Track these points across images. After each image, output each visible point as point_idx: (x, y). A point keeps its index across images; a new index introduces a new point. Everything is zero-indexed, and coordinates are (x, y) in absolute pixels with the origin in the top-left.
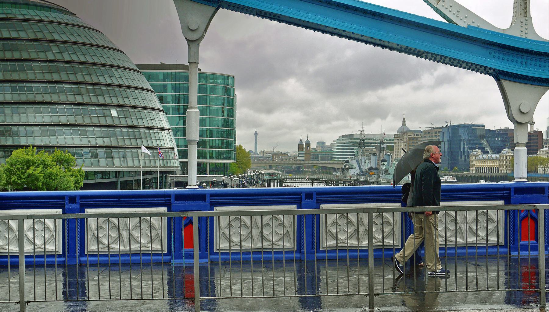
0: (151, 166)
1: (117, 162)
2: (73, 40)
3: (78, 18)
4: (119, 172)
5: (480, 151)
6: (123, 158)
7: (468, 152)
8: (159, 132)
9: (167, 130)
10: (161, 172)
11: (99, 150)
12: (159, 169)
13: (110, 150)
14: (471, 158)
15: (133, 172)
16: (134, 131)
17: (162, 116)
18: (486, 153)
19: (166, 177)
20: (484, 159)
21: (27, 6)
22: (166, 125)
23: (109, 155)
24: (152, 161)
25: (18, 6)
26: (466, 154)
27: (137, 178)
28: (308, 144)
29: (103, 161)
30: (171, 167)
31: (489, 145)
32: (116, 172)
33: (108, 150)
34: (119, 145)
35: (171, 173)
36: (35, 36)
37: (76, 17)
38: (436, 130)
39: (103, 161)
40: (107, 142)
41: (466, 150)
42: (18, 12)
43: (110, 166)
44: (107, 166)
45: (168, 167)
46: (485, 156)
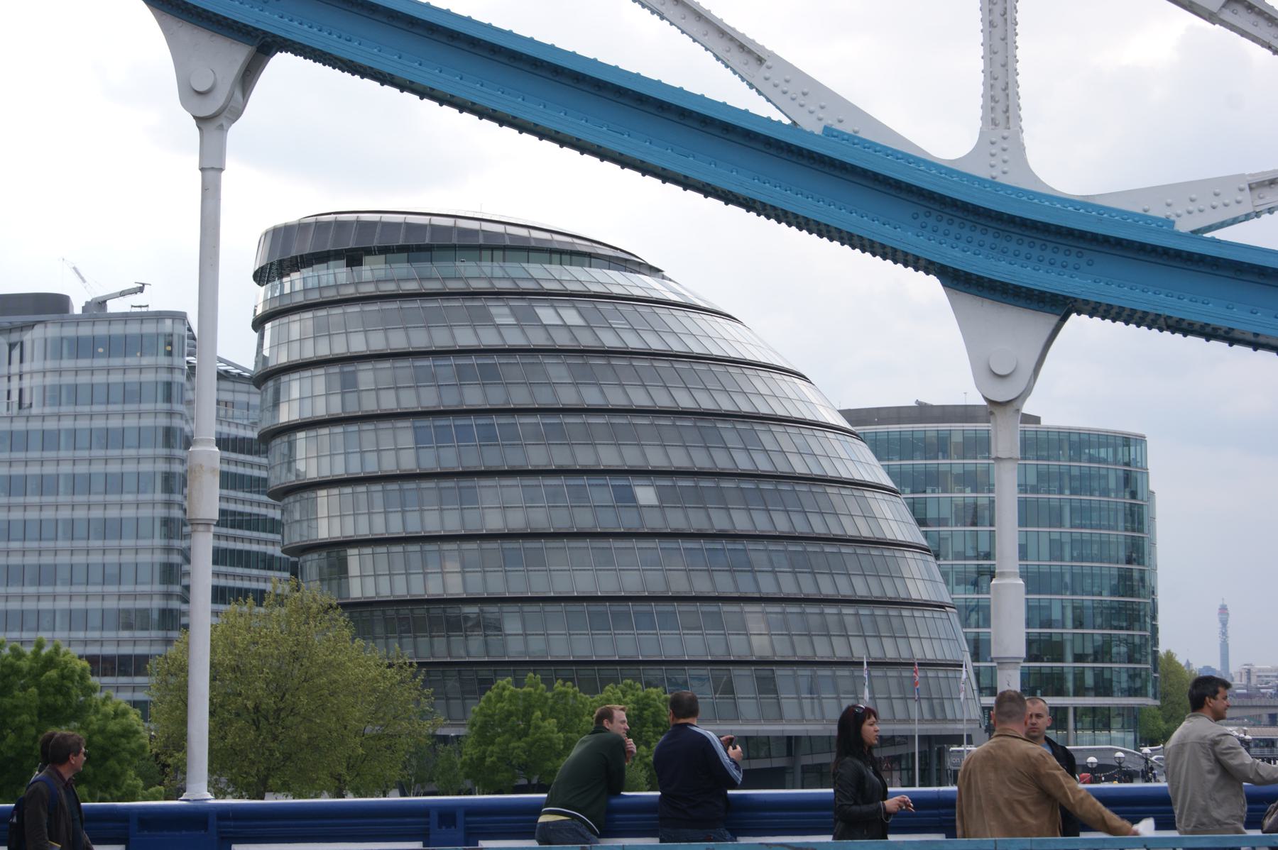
0: (893, 720)
1: (789, 705)
2: (656, 345)
3: (670, 280)
4: (798, 738)
6: (809, 696)
8: (917, 614)
10: (926, 739)
11: (737, 671)
12: (917, 729)
13: (769, 673)
16: (840, 614)
19: (941, 755)
23: (767, 687)
24: (898, 705)
25: (498, 254)
29: (748, 705)
30: (955, 721)
32: (789, 738)
33: (765, 671)
34: (795, 655)
35: (957, 739)
36: (547, 339)
37: (664, 277)
39: (748, 705)
40: (761, 646)
42: (498, 272)
43: (768, 720)
44: (764, 718)
45: (945, 720)
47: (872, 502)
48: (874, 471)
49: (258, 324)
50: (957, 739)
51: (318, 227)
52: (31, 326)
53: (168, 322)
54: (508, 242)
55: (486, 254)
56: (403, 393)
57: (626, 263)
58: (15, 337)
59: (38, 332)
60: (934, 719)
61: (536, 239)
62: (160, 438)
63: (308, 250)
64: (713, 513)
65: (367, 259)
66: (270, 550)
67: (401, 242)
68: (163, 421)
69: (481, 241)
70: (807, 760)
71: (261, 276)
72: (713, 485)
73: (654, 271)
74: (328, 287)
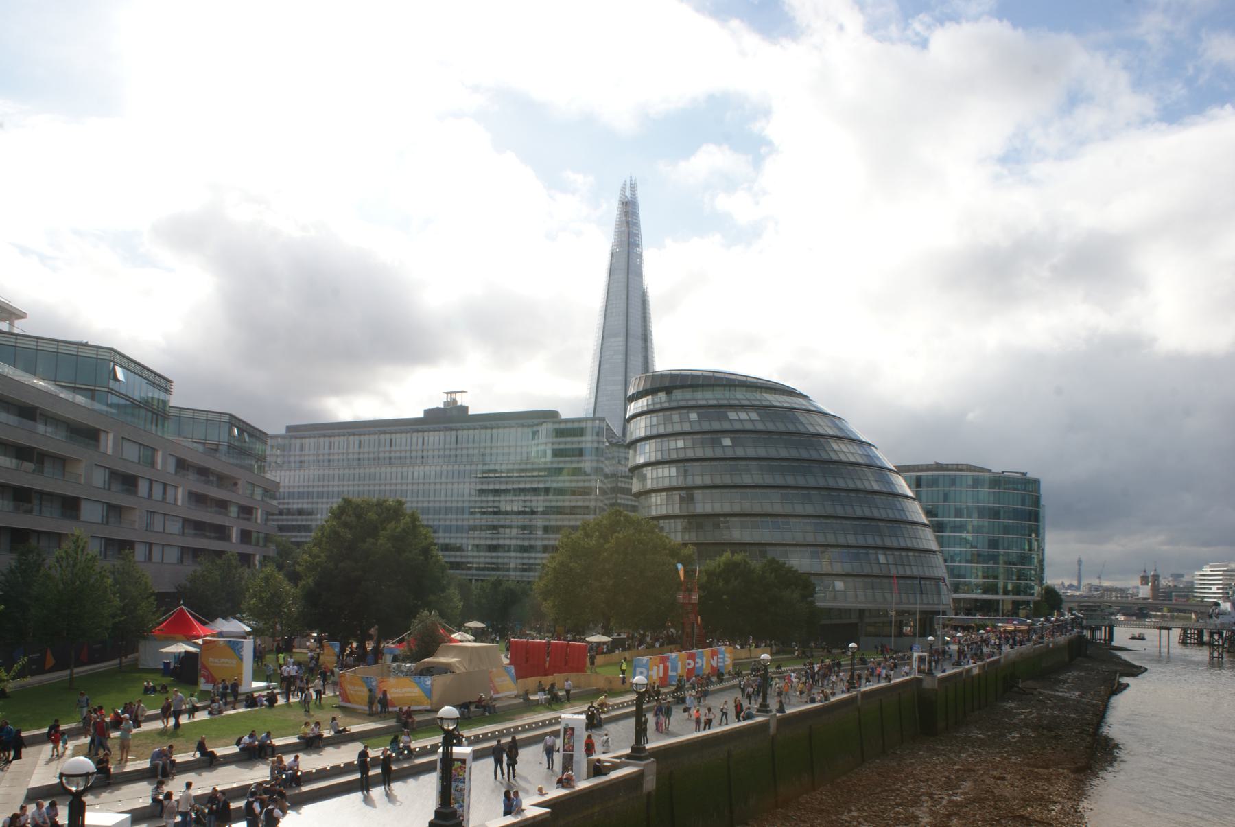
9: (934, 552)
15: (882, 611)
21: (744, 389)
22: (934, 546)
32: (860, 610)
35: (938, 613)
37: (810, 400)
47: (907, 504)
52: (541, 424)
53: (597, 422)
54: (737, 383)
55: (727, 388)
56: (688, 451)
57: (790, 392)
58: (535, 429)
59: (544, 426)
61: (750, 382)
65: (675, 391)
67: (689, 383)
69: (724, 382)
72: (826, 493)
73: (805, 397)
74: (657, 403)
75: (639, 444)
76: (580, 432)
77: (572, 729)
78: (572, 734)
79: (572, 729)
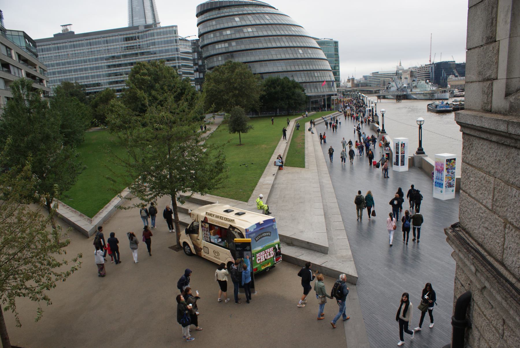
2: (276, 22)
5: (453, 76)
7: (446, 77)
10: (328, 95)
14: (448, 80)
17: (327, 63)
18: (456, 76)
19: (330, 98)
20: (456, 80)
24: (322, 89)
26: (445, 78)
27: (324, 98)
28: (353, 79)
31: (458, 72)
38: (427, 66)
41: (445, 75)
45: (332, 91)
46: (456, 78)
48: (317, 46)
49: (198, 25)
50: (333, 95)
51: (207, 4)
59: (150, 32)
60: (330, 91)
62: (176, 50)
63: (209, 8)
64: (286, 55)
66: (191, 71)
68: (176, 47)
70: (311, 100)
71: (197, 16)
75: (205, 35)
76: (175, 33)
77: (404, 144)
78: (404, 146)
79: (404, 144)
